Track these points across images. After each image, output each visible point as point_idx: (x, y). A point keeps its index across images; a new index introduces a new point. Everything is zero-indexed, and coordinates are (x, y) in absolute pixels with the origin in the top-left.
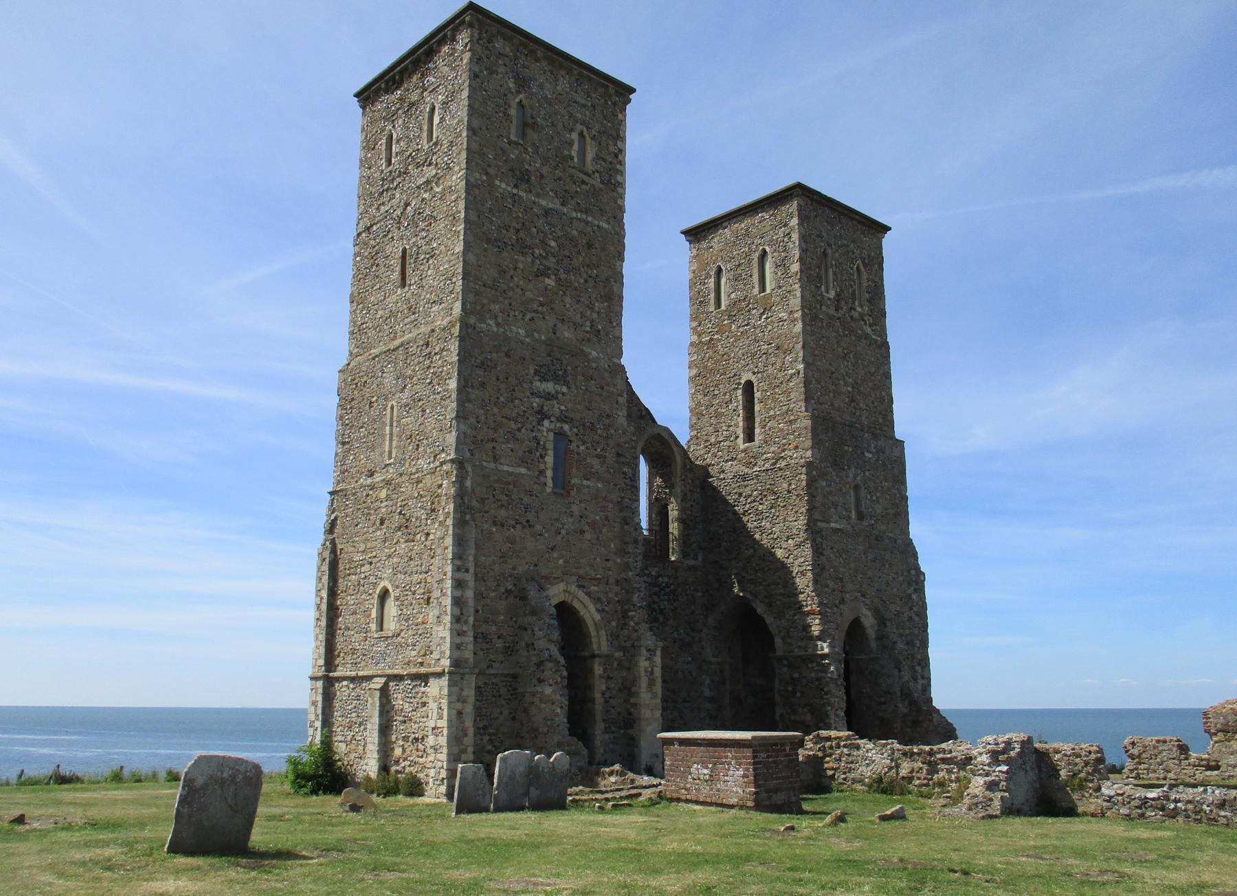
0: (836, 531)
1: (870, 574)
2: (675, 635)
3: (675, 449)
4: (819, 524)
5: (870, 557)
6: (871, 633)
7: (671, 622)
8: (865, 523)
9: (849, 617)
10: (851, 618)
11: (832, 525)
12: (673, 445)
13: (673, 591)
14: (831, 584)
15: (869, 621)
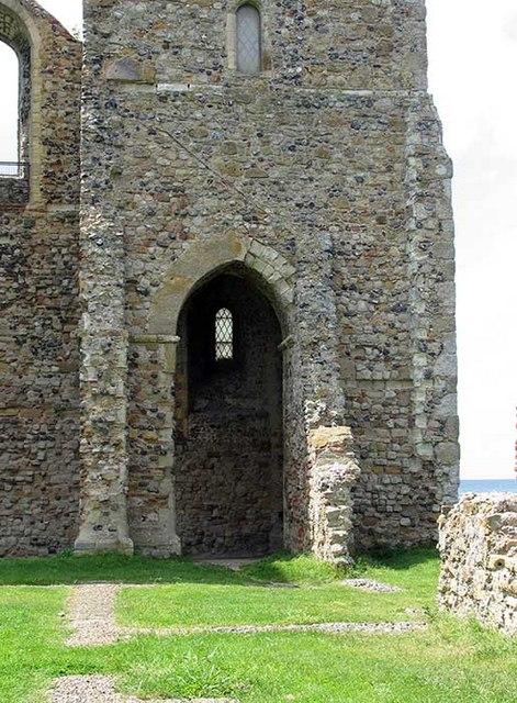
0: (163, 98)
1: (275, 173)
2: (22, 330)
3: (29, 22)
4: (132, 89)
5: (278, 139)
6: (286, 292)
7: (13, 308)
8: (270, 74)
9: (194, 261)
10: (208, 265)
11: (162, 87)
12: (24, 14)
13: (23, 260)
14: (145, 201)
15: (272, 266)
